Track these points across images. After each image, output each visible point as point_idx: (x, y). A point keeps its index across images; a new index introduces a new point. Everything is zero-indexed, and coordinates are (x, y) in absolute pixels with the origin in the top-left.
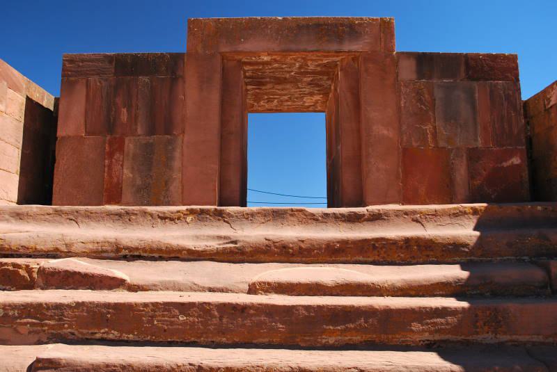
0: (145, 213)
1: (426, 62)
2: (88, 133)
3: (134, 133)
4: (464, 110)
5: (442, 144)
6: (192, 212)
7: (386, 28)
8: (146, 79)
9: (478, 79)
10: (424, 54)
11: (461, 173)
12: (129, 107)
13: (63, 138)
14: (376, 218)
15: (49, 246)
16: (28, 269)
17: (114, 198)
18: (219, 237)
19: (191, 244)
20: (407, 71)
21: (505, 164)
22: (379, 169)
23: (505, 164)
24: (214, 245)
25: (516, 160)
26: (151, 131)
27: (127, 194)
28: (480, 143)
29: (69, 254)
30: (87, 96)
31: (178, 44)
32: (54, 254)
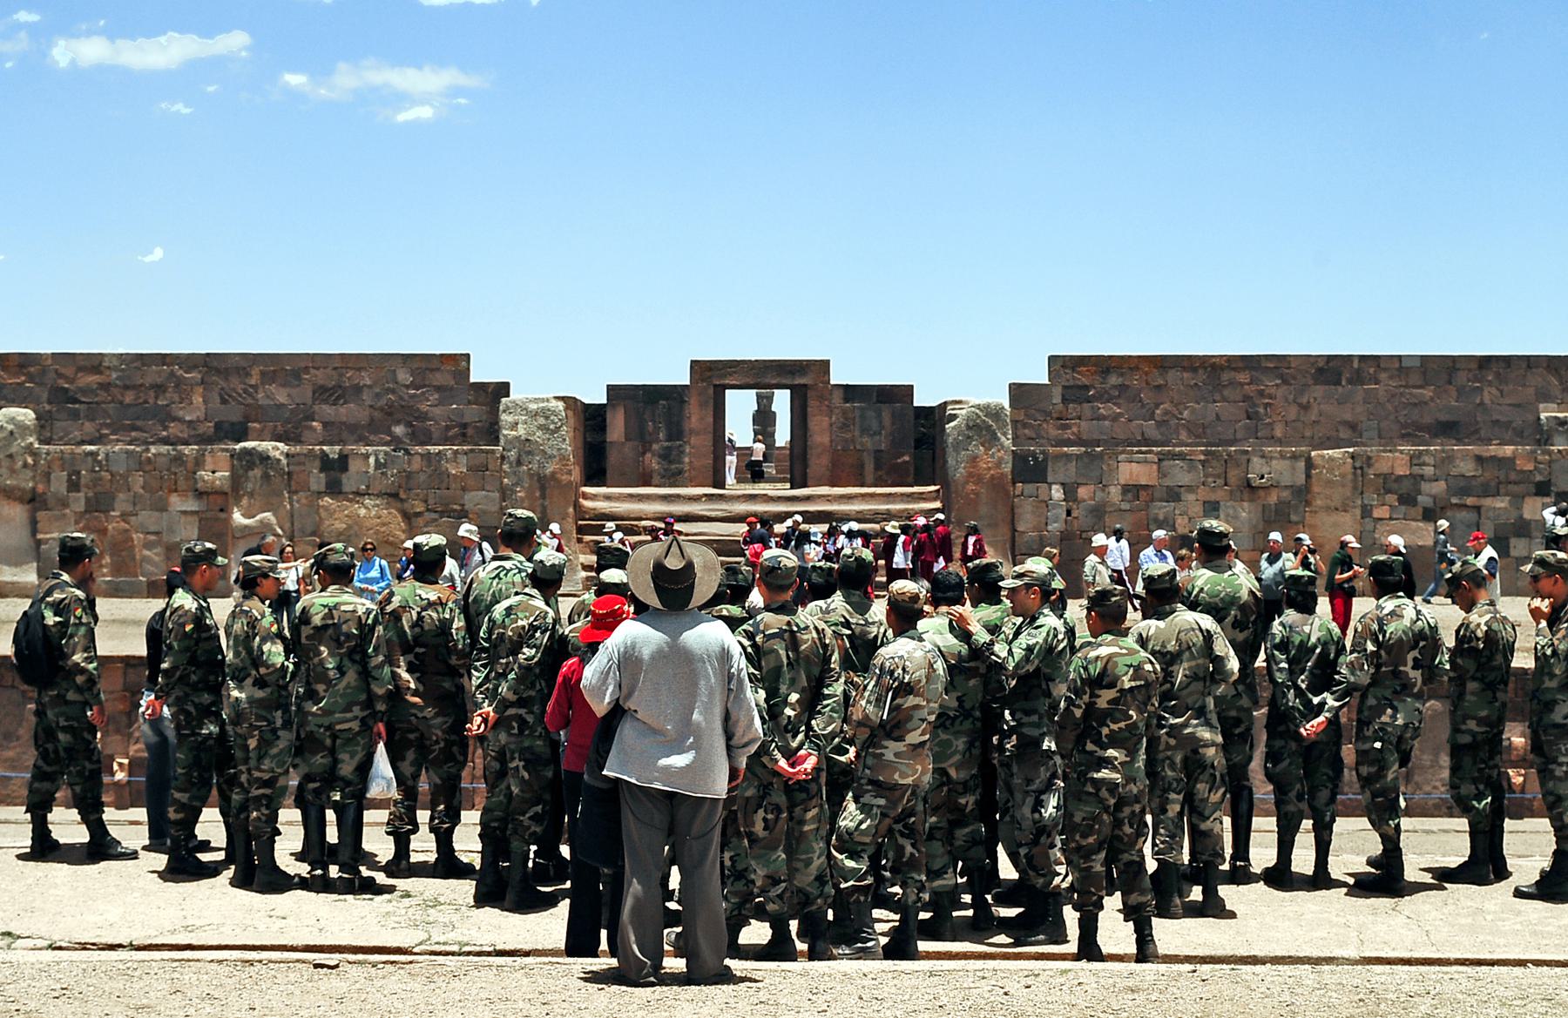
0: (678, 496)
1: (851, 392)
2: (626, 440)
3: (657, 441)
4: (875, 425)
5: (858, 447)
6: (706, 495)
7: (824, 366)
8: (664, 402)
9: (885, 403)
10: (847, 386)
11: (869, 467)
12: (654, 421)
13: (611, 442)
14: (808, 499)
15: (638, 515)
16: (636, 526)
17: (647, 483)
18: (722, 510)
19: (708, 514)
20: (837, 398)
21: (899, 461)
22: (818, 463)
23: (899, 461)
24: (719, 514)
25: (907, 458)
26: (669, 438)
27: (656, 479)
28: (883, 447)
29: (647, 519)
30: (625, 413)
31: (685, 380)
32: (641, 519)
